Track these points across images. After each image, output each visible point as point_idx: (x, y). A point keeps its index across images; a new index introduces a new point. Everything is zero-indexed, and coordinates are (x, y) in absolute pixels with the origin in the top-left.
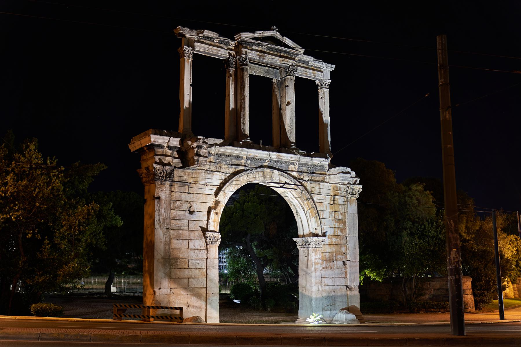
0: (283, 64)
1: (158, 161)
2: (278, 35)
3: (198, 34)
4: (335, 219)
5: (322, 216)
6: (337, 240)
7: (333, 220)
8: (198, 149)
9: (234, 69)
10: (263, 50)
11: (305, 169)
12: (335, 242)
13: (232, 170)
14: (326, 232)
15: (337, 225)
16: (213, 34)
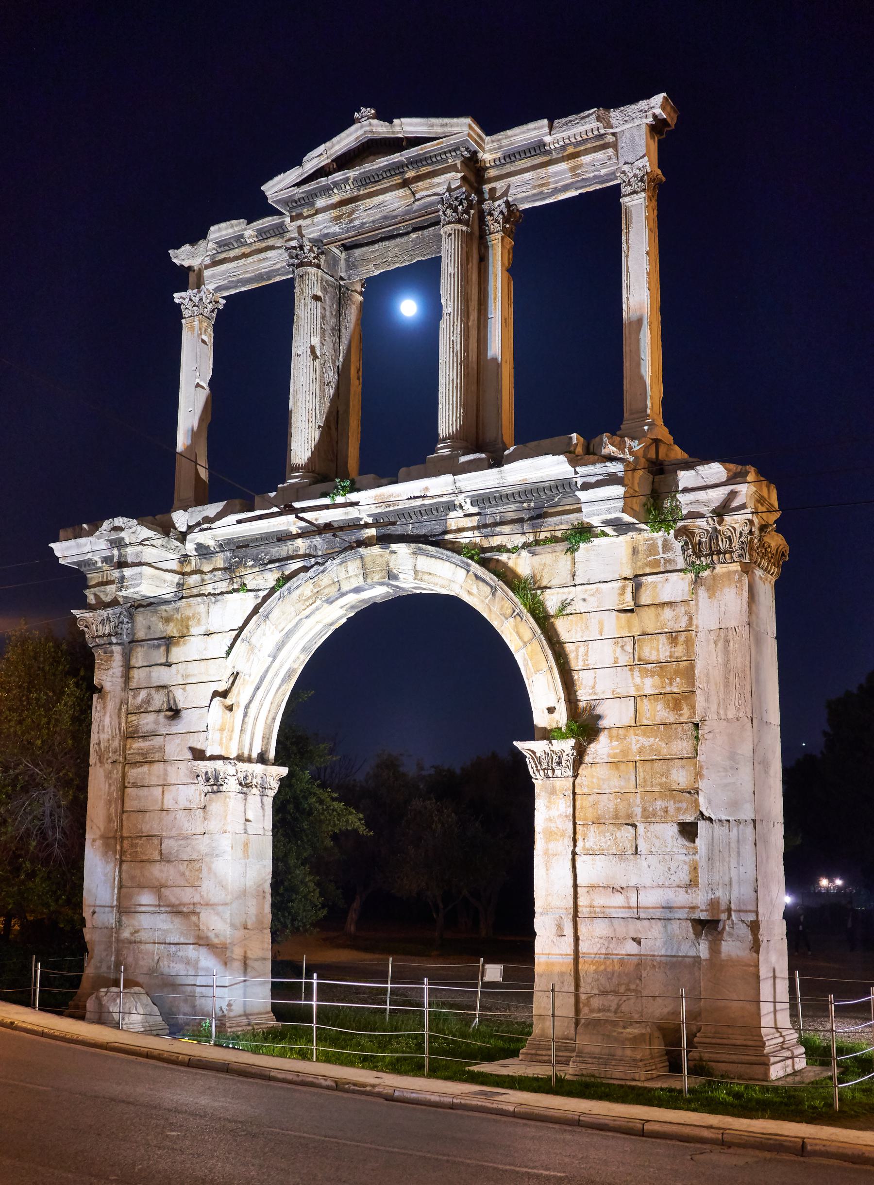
0: (417, 203)
1: (93, 602)
4: (639, 664)
6: (647, 742)
7: (631, 670)
8: (119, 550)
10: (347, 195)
11: (510, 510)
12: (640, 752)
15: (649, 685)
16: (232, 226)
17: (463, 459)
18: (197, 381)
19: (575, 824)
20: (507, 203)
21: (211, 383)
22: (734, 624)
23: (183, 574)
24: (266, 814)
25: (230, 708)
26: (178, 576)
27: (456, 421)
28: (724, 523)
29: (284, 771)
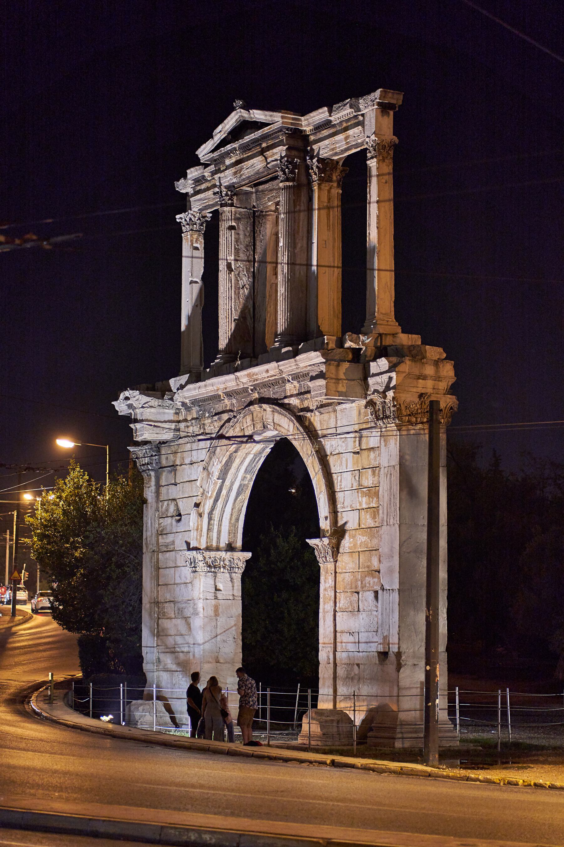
2: (244, 114)
5: (339, 487)
7: (358, 492)
14: (346, 523)
15: (364, 502)
17: (284, 350)
18: (190, 279)
19: (335, 592)
20: (320, 160)
21: (203, 278)
22: (393, 463)
23: (179, 422)
24: (235, 585)
25: (200, 515)
26: (174, 424)
27: (285, 322)
28: (387, 398)
29: (249, 555)
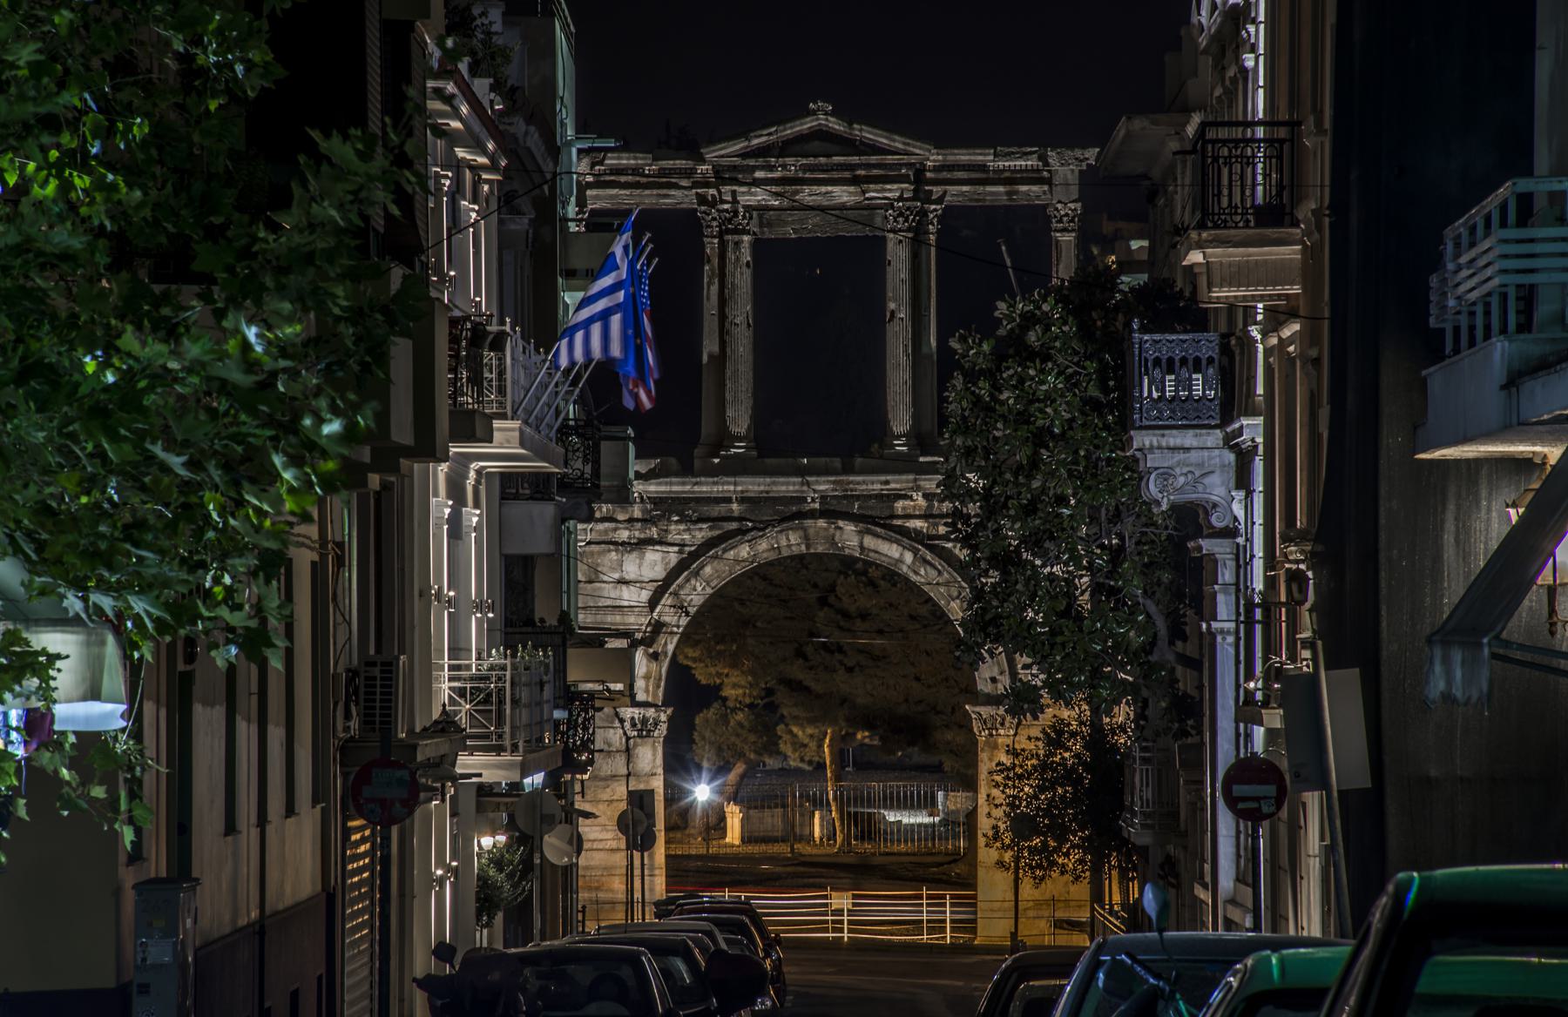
2: (836, 125)
3: (593, 165)
9: (716, 241)
13: (702, 533)
